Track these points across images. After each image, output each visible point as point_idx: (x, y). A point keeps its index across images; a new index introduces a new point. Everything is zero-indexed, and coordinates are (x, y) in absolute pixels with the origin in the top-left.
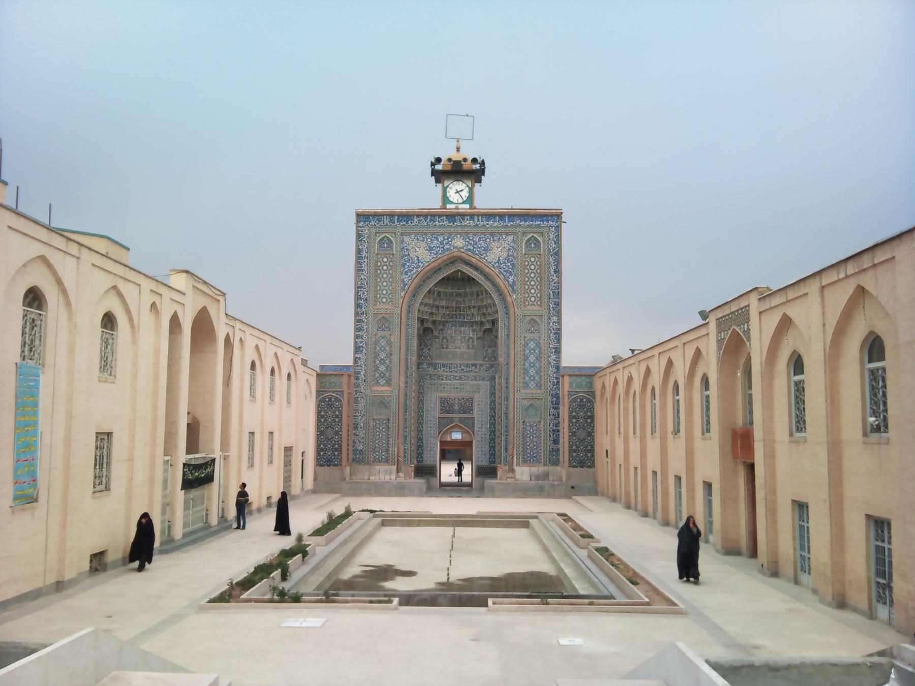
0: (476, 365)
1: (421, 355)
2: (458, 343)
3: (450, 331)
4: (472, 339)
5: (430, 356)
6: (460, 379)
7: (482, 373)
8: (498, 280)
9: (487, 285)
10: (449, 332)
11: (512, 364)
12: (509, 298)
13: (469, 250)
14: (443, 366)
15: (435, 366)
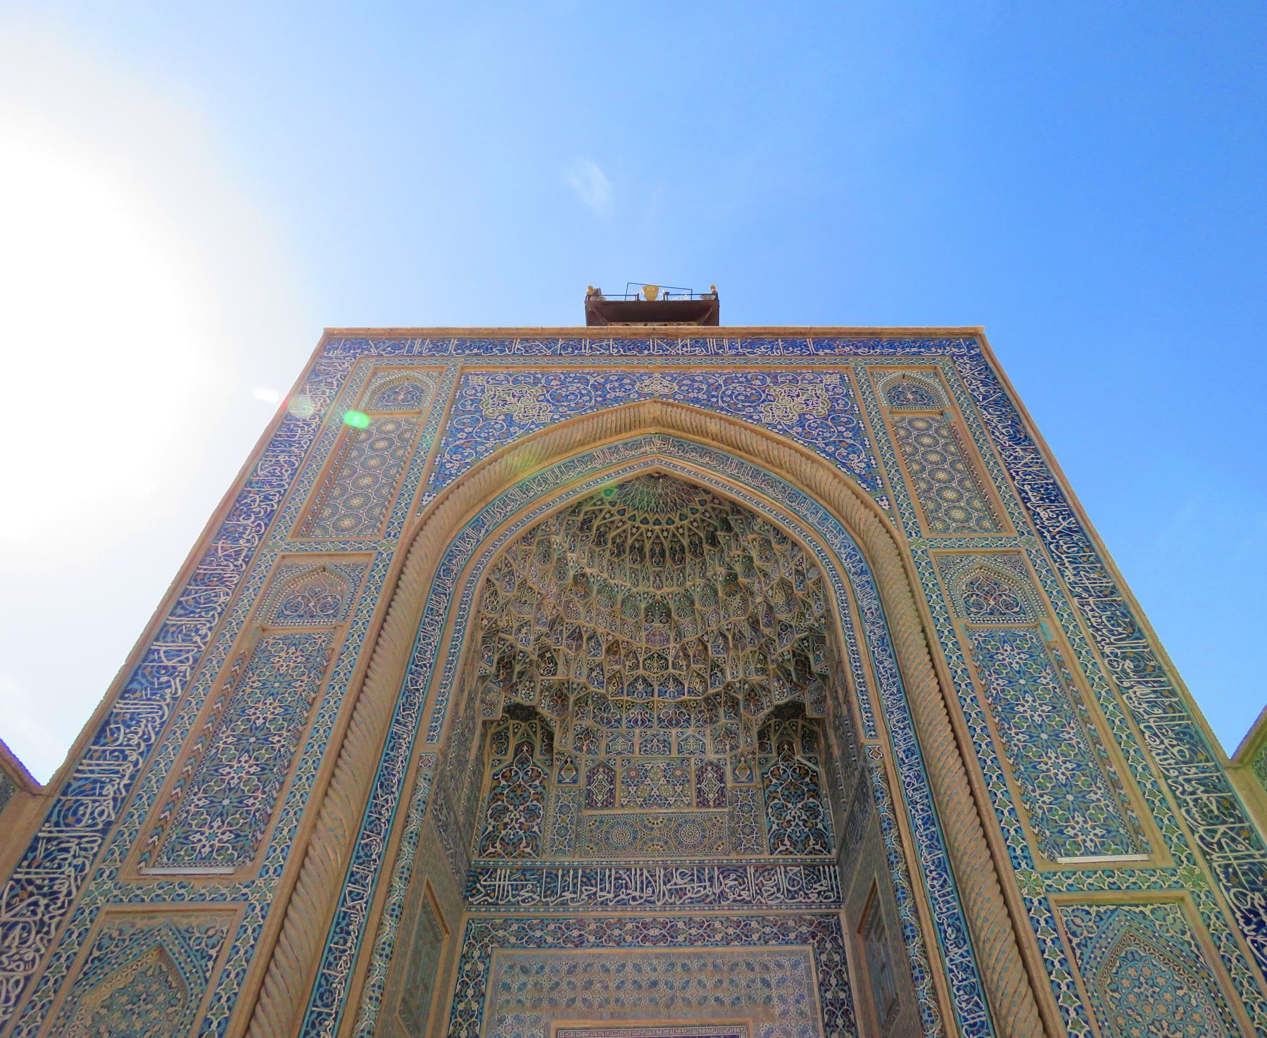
0: (739, 871)
1: (491, 838)
2: (657, 784)
3: (624, 744)
4: (718, 768)
5: (534, 836)
6: (670, 934)
7: (776, 907)
8: (807, 468)
9: (767, 505)
10: (620, 745)
11: (940, 738)
12: (861, 516)
13: (696, 400)
14: (588, 880)
15: (550, 882)
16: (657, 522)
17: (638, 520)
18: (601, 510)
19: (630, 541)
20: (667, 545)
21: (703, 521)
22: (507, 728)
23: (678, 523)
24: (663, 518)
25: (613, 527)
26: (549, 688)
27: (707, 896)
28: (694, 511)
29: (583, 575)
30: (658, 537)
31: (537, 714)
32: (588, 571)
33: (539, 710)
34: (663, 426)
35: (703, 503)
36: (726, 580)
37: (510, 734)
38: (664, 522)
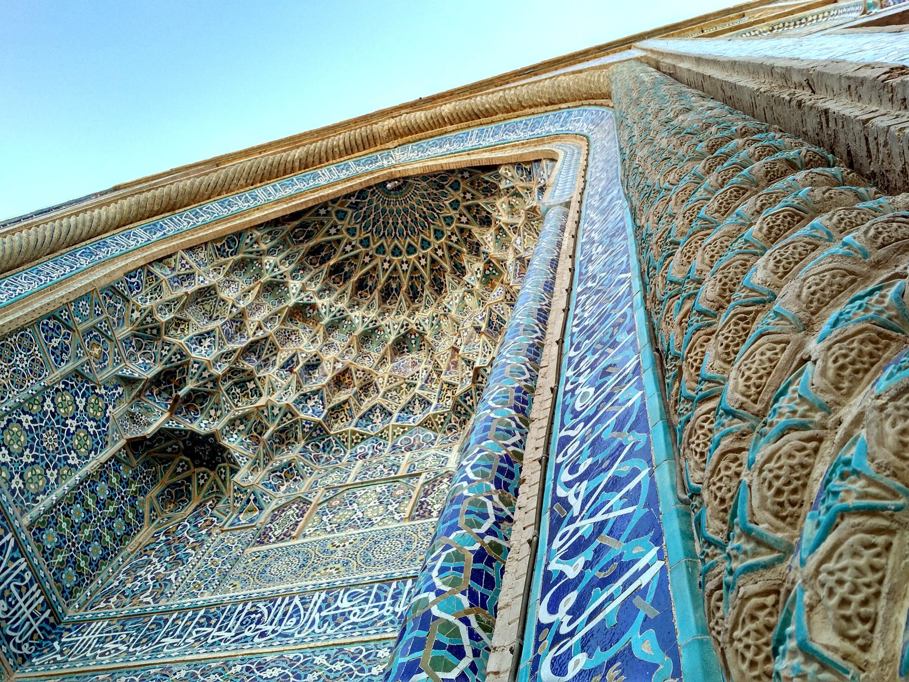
16: (411, 250)
17: (389, 250)
18: (339, 241)
19: (383, 280)
20: (426, 274)
21: (462, 230)
22: (189, 479)
23: (435, 244)
24: (416, 241)
25: (359, 263)
26: (244, 418)
27: (383, 617)
28: (449, 220)
29: (313, 306)
30: (415, 269)
31: (224, 449)
32: (319, 302)
33: (225, 442)
34: (402, 137)
35: (455, 205)
36: (485, 276)
37: (193, 488)
38: (418, 247)
